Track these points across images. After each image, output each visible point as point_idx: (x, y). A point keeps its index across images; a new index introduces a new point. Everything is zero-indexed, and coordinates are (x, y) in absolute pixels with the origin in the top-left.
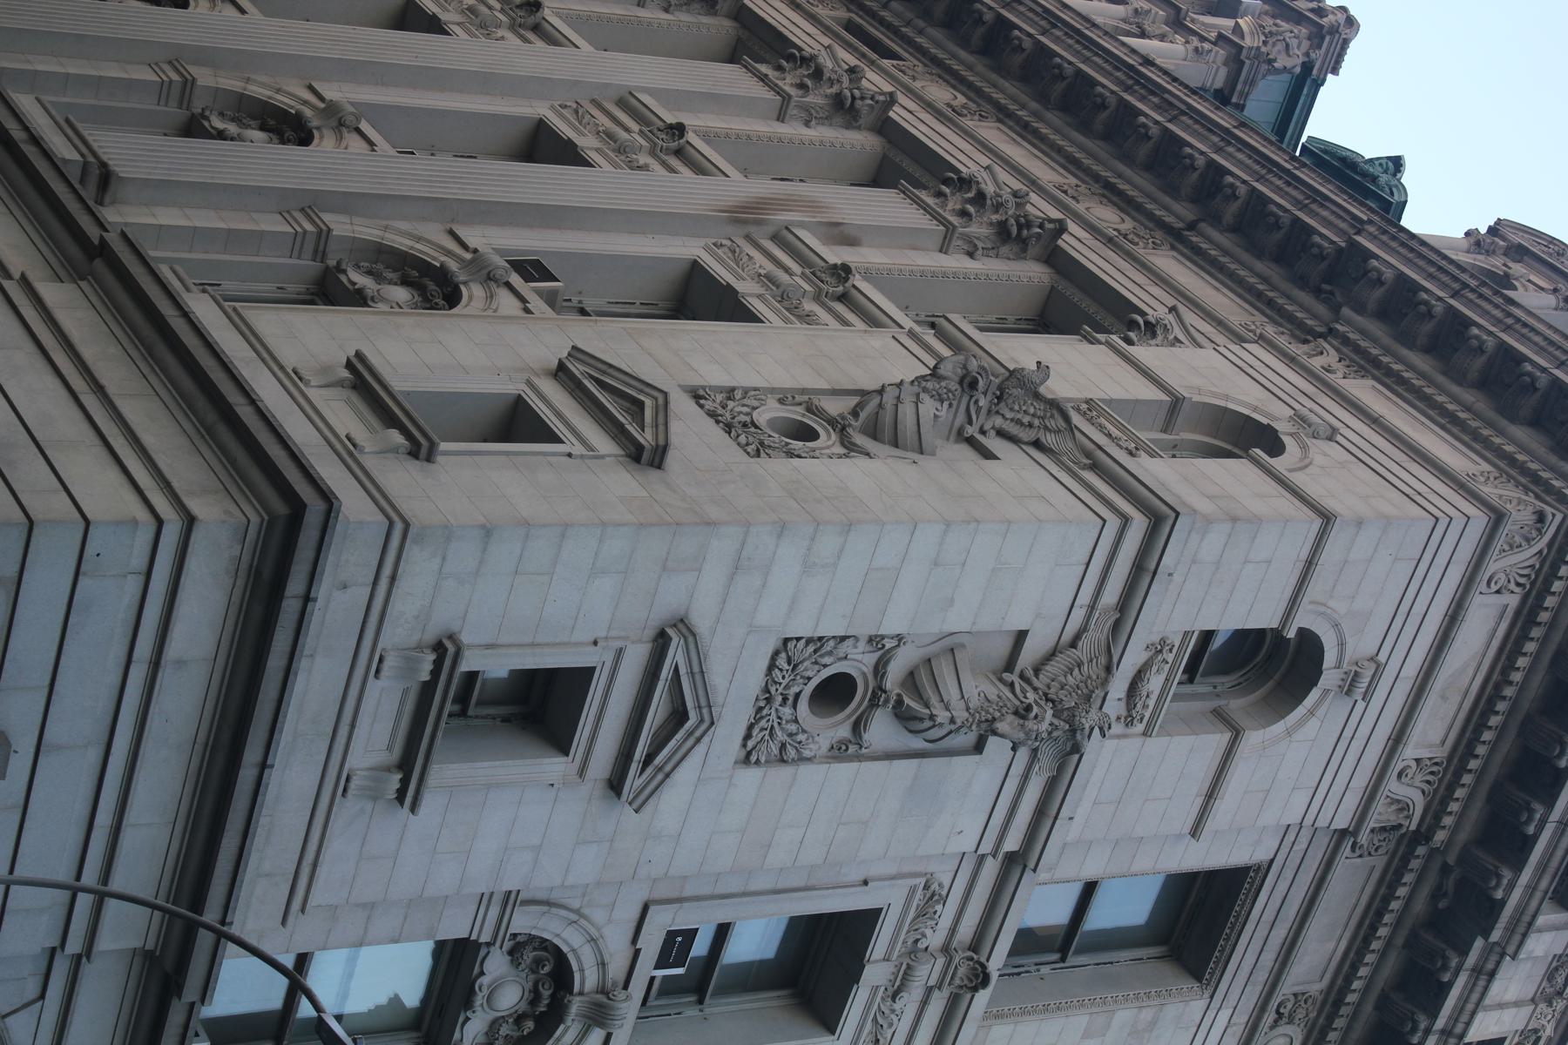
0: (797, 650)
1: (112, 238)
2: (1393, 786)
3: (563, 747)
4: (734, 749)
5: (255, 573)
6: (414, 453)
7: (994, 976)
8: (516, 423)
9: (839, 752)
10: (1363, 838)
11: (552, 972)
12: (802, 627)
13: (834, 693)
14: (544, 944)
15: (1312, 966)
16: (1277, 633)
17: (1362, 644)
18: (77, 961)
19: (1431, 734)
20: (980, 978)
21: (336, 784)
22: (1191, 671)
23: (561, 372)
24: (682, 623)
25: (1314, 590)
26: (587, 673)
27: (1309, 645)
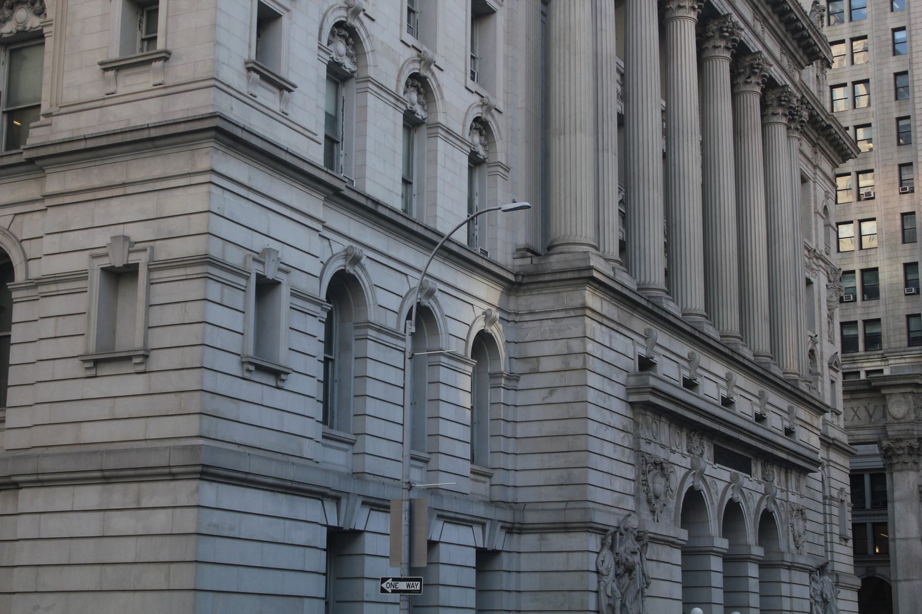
5: (229, 146)
6: (166, 59)
18: (325, 227)
21: (283, 117)
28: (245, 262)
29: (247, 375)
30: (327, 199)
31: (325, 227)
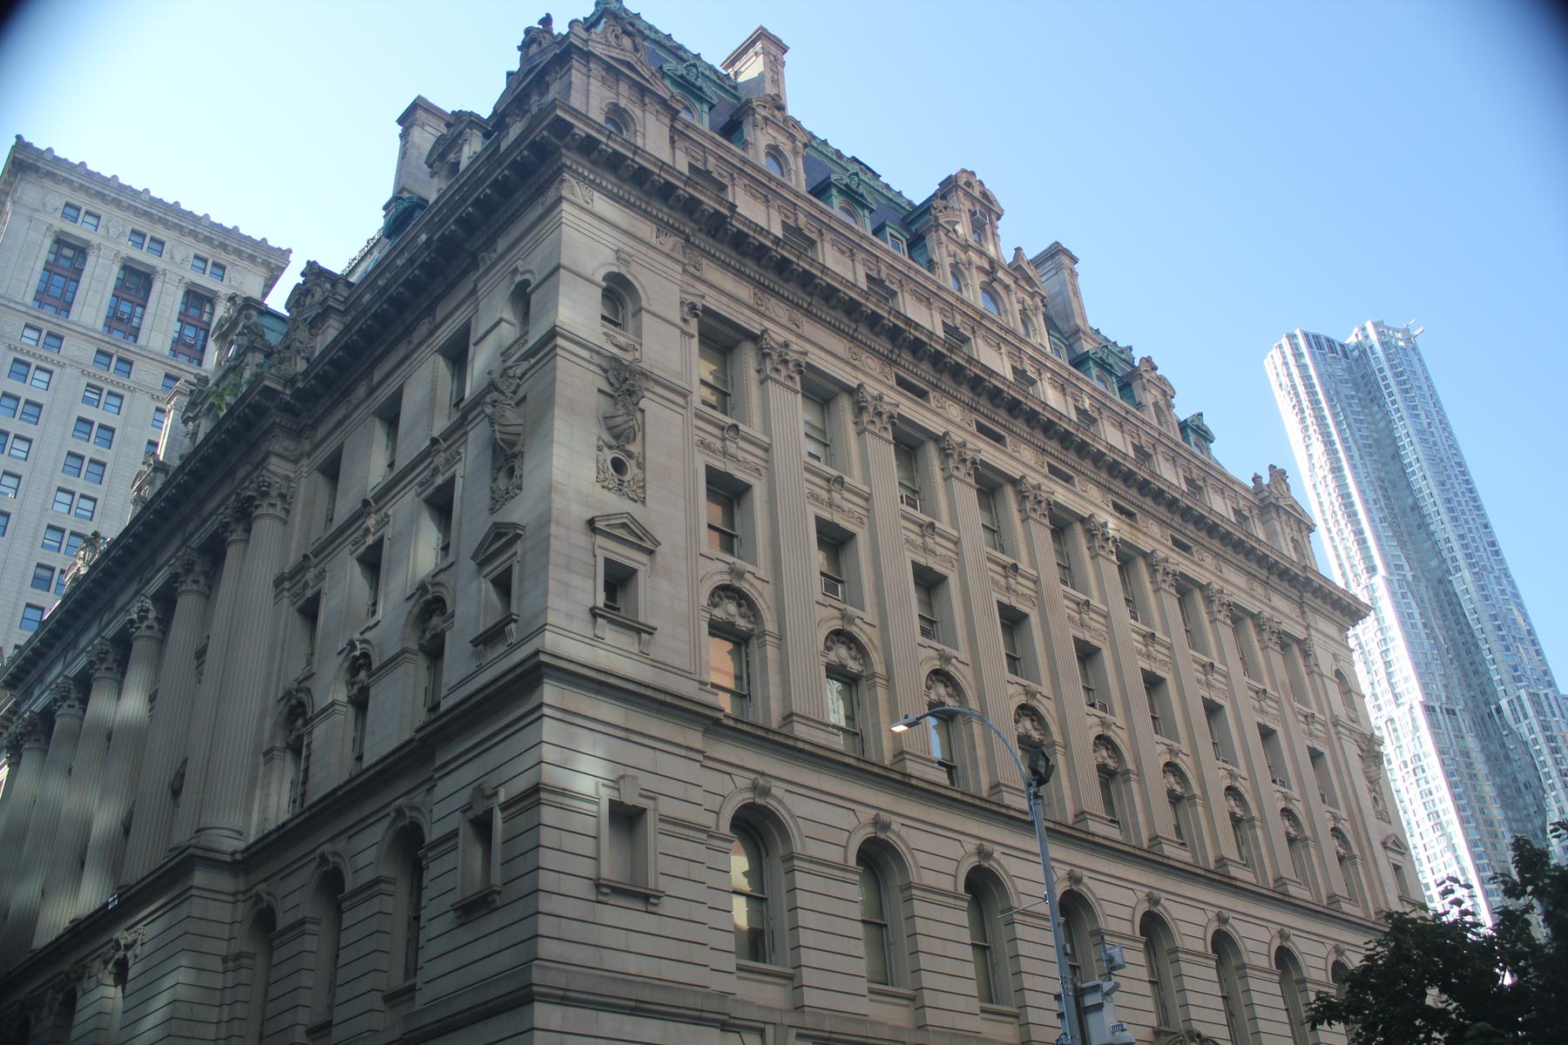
0: (602, 477)
1: (418, 736)
3: (635, 571)
4: (639, 505)
8: (503, 585)
9: (641, 466)
12: (593, 475)
13: (618, 466)
15: (744, 292)
16: (604, 290)
17: (610, 256)
18: (706, 757)
19: (646, 230)
22: (616, 324)
23: (481, 565)
24: (591, 522)
25: (588, 272)
26: (607, 561)
27: (610, 277)
28: (597, 790)
29: (601, 898)
30: (706, 732)
31: (706, 757)
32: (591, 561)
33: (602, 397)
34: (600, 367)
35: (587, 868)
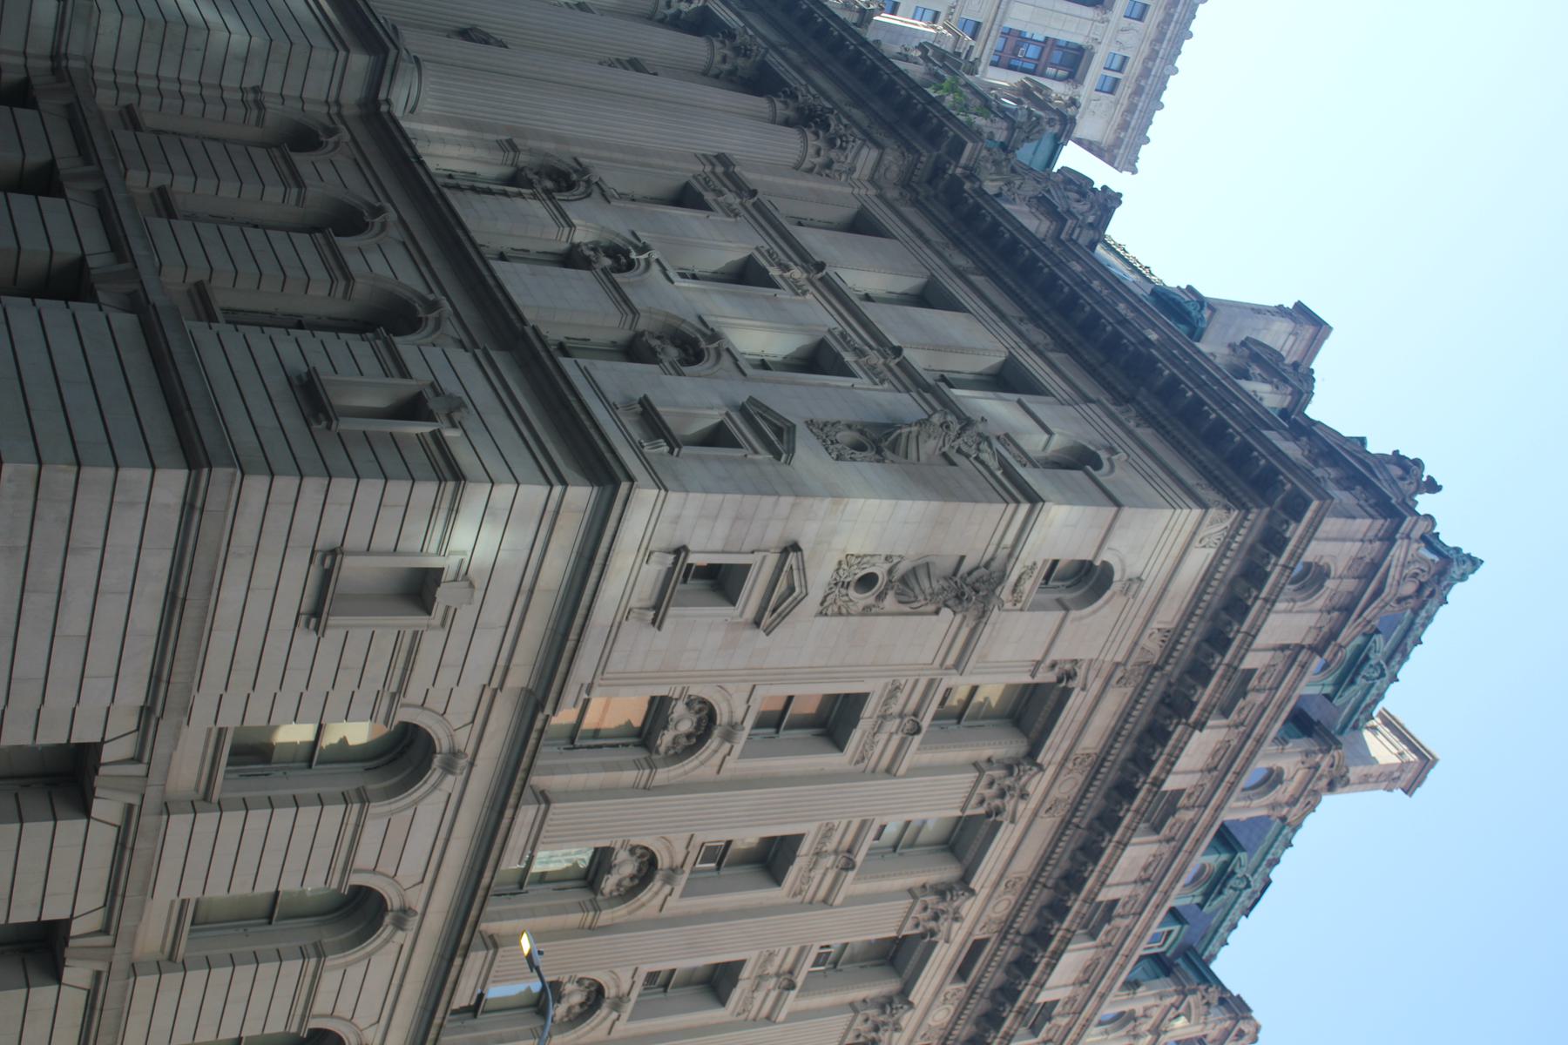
2: (1144, 641)
7: (924, 730)
8: (717, 437)
10: (1129, 667)
11: (707, 718)
14: (703, 701)
16: (1091, 563)
17: (1135, 568)
19: (1168, 615)
20: (917, 730)
22: (1047, 578)
23: (743, 410)
25: (1113, 542)
27: (1107, 570)
29: (318, 557)
32: (747, 547)
33: (953, 562)
34: (992, 559)
35: (357, 538)
